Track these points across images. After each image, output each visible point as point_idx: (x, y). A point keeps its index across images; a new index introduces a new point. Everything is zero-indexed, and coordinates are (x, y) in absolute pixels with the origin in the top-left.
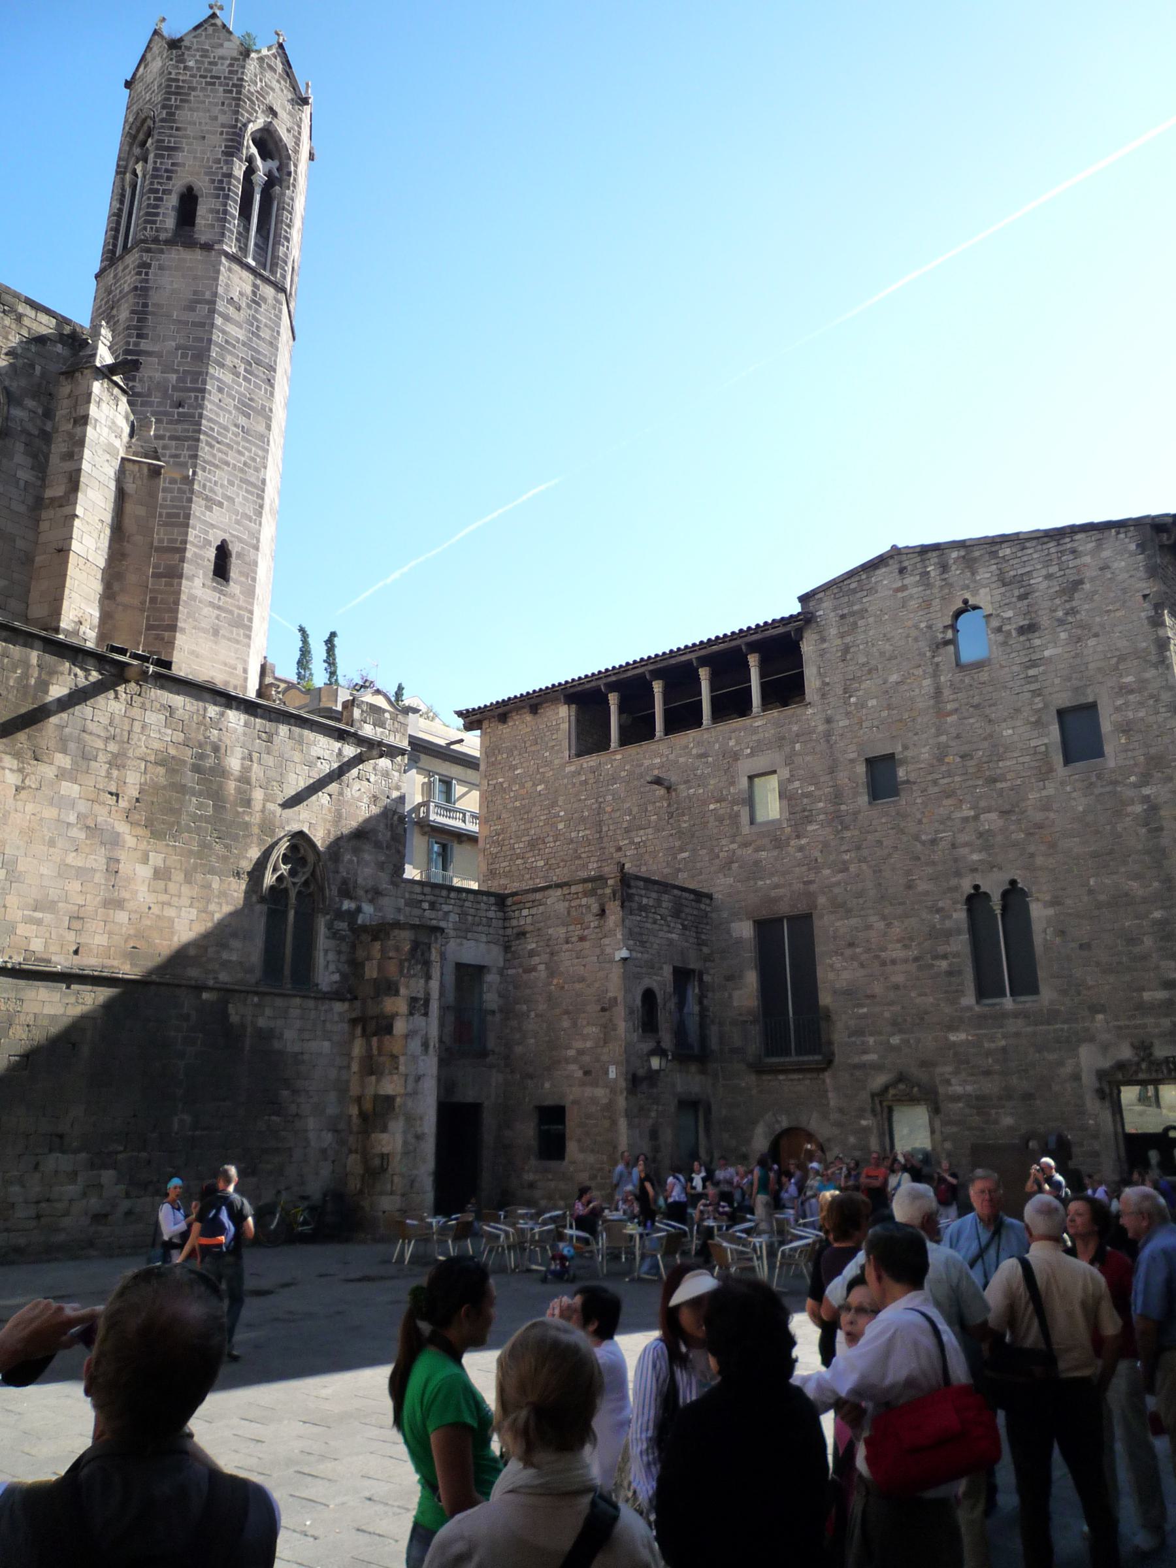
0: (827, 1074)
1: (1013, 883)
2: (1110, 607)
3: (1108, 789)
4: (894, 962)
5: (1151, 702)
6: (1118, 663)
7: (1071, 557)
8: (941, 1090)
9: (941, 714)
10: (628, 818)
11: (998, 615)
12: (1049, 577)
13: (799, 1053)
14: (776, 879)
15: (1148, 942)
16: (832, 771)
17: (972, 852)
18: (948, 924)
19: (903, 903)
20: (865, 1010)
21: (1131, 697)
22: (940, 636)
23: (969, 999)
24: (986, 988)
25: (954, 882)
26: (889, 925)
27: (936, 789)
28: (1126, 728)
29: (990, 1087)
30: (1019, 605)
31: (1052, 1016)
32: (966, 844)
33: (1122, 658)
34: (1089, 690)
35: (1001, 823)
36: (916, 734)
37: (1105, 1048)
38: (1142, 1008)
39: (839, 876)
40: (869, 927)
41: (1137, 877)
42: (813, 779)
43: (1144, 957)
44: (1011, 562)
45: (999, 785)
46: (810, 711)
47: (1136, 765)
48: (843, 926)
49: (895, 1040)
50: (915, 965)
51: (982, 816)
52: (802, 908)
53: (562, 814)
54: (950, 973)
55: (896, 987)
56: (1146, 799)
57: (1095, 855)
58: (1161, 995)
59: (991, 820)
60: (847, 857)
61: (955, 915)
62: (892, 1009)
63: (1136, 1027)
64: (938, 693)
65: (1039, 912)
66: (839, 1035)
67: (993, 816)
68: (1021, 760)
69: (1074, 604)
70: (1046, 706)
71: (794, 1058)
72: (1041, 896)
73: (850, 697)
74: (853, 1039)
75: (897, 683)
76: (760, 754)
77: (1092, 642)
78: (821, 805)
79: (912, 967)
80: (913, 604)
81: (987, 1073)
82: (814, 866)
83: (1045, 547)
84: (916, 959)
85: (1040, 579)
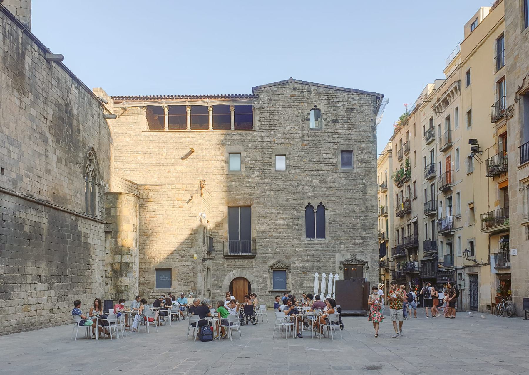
0: (253, 259)
1: (321, 203)
2: (361, 120)
3: (353, 178)
4: (279, 225)
5: (369, 154)
6: (361, 139)
7: (351, 100)
8: (292, 265)
9: (303, 144)
10: (173, 160)
11: (326, 114)
12: (344, 105)
13: (242, 252)
14: (238, 192)
15: (359, 225)
16: (262, 157)
17: (309, 192)
18: (299, 214)
19: (285, 206)
20: (269, 239)
21: (363, 151)
22: (306, 116)
23: (304, 238)
24: (310, 234)
25: (302, 201)
26: (279, 213)
27: (299, 170)
28: (360, 160)
29: (308, 265)
30: (333, 112)
31: (329, 245)
32: (308, 190)
33: (362, 138)
34: (352, 146)
35: (319, 184)
36: (294, 150)
37: (343, 255)
38: (355, 244)
39: (263, 194)
40: (272, 213)
41: (359, 206)
42: (254, 158)
43: (357, 230)
44: (332, 96)
45: (320, 172)
46: (255, 133)
47: (362, 172)
48: (263, 211)
49: (278, 250)
50: (287, 226)
51: (313, 181)
52: (248, 203)
53: (140, 153)
54: (298, 230)
55: (280, 233)
56: (364, 183)
57: (347, 198)
58: (361, 241)
59: (316, 183)
60: (266, 188)
61: (301, 212)
62: (277, 239)
63: (352, 250)
64: (303, 136)
65: (328, 214)
66: (258, 247)
67: (317, 181)
68: (328, 165)
69: (351, 116)
70: (338, 149)
71: (240, 254)
72: (329, 209)
73: (271, 131)
74: (263, 249)
75: (289, 130)
76: (234, 145)
77: (354, 130)
78: (257, 168)
79: (286, 227)
80: (297, 103)
81: (307, 261)
82: (253, 189)
83: (344, 94)
84: (287, 225)
85: (341, 105)
